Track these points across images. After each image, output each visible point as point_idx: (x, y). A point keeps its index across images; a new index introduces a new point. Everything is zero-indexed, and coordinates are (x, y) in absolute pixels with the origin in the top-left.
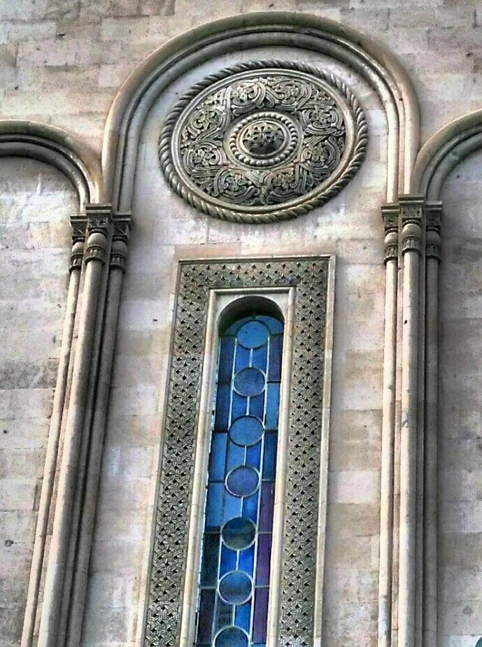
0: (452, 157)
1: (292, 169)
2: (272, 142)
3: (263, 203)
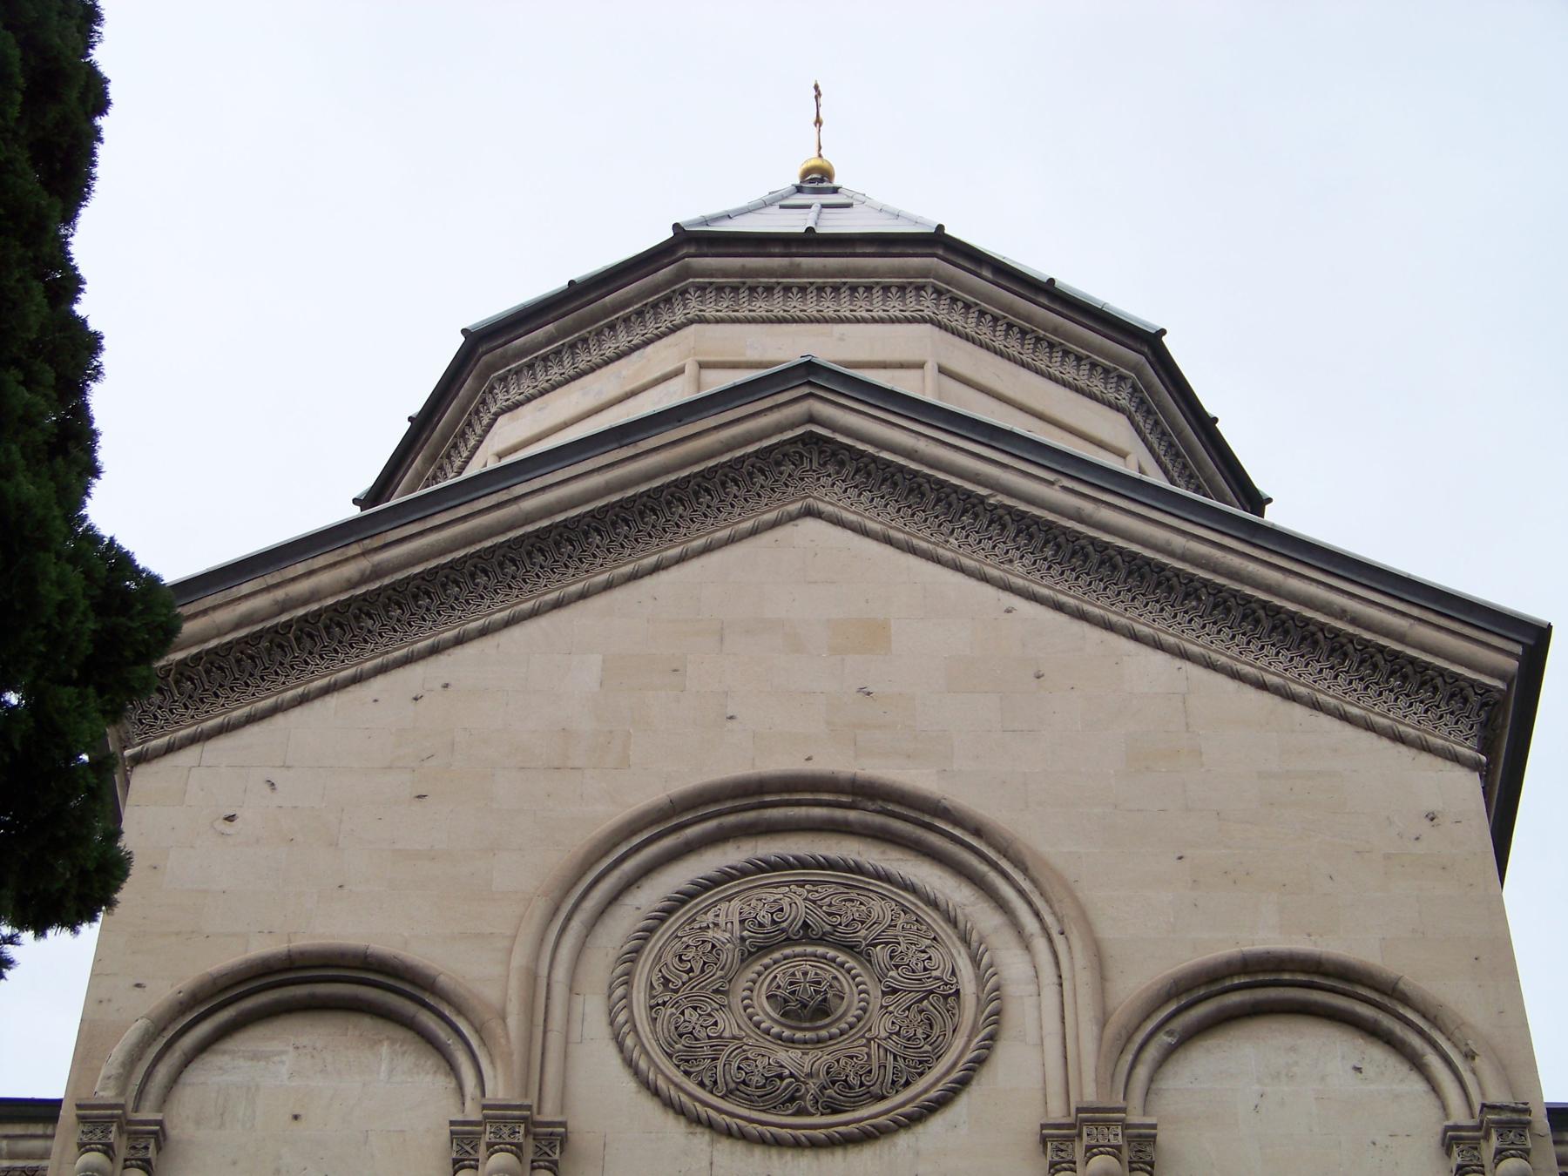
0: (1164, 1039)
1: (866, 1050)
2: (825, 1000)
3: (812, 1111)
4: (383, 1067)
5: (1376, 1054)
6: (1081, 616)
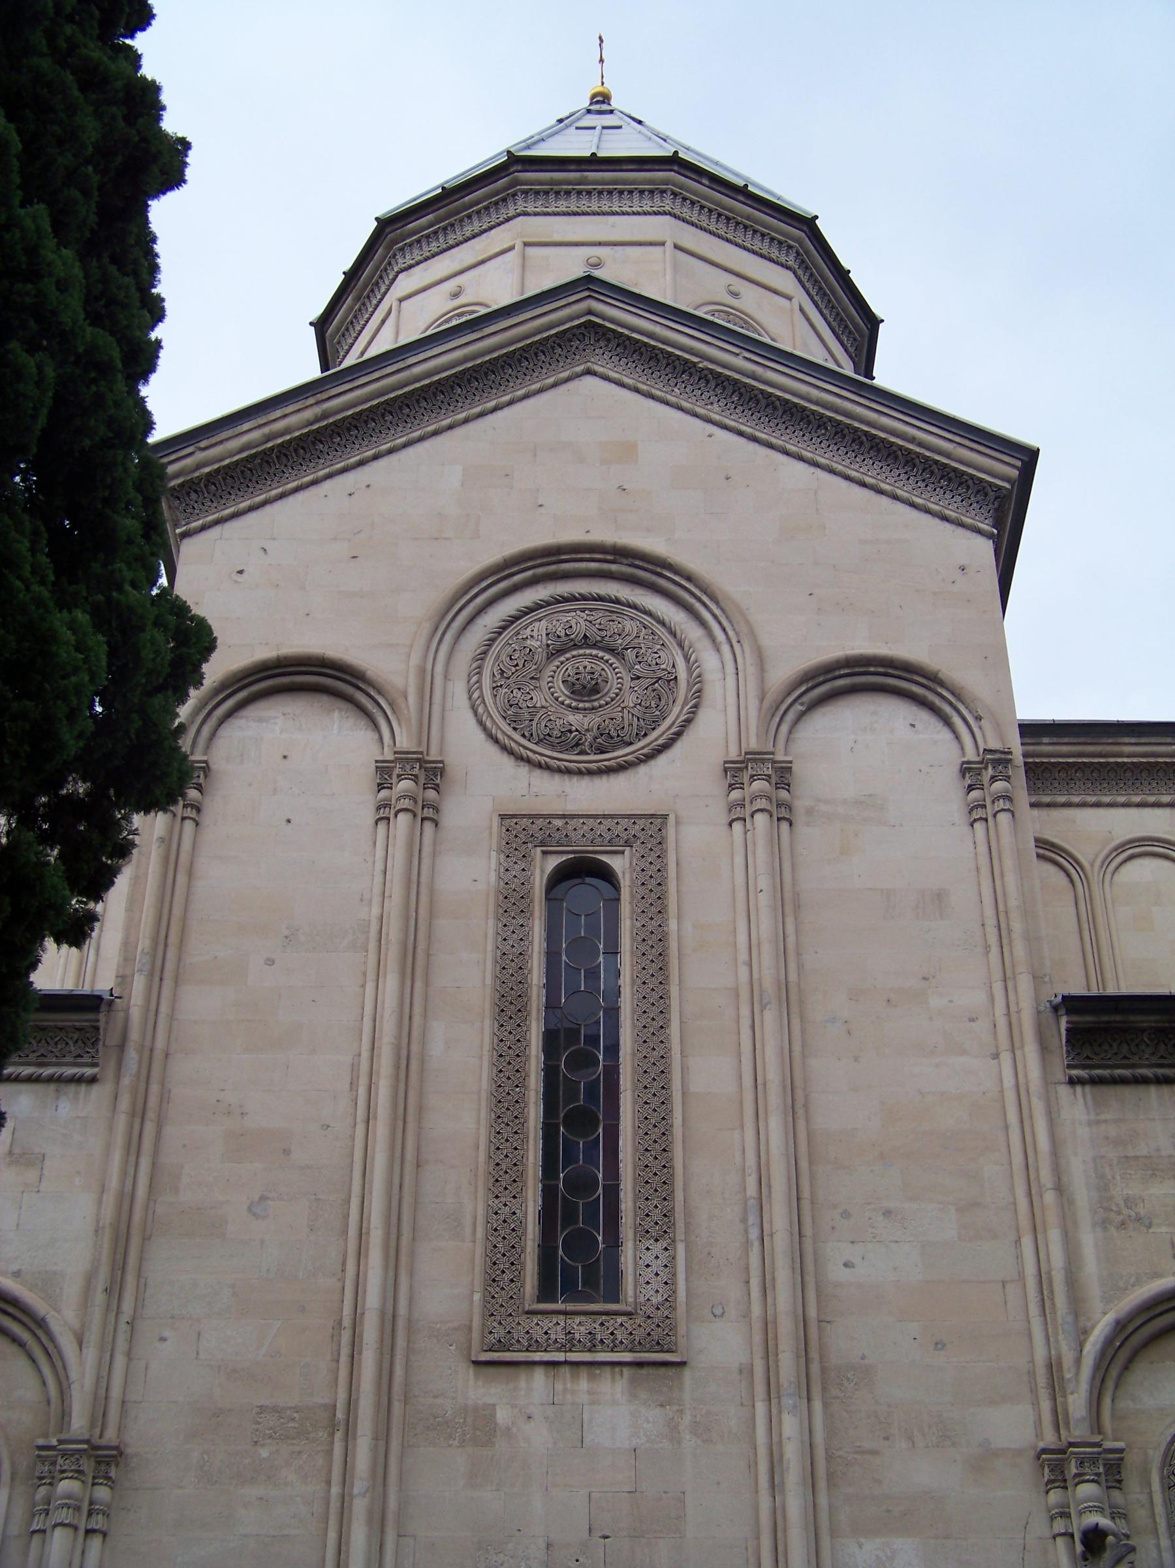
0: (798, 708)
1: (621, 714)
3: (589, 752)
4: (336, 726)
5: (924, 716)
6: (754, 439)
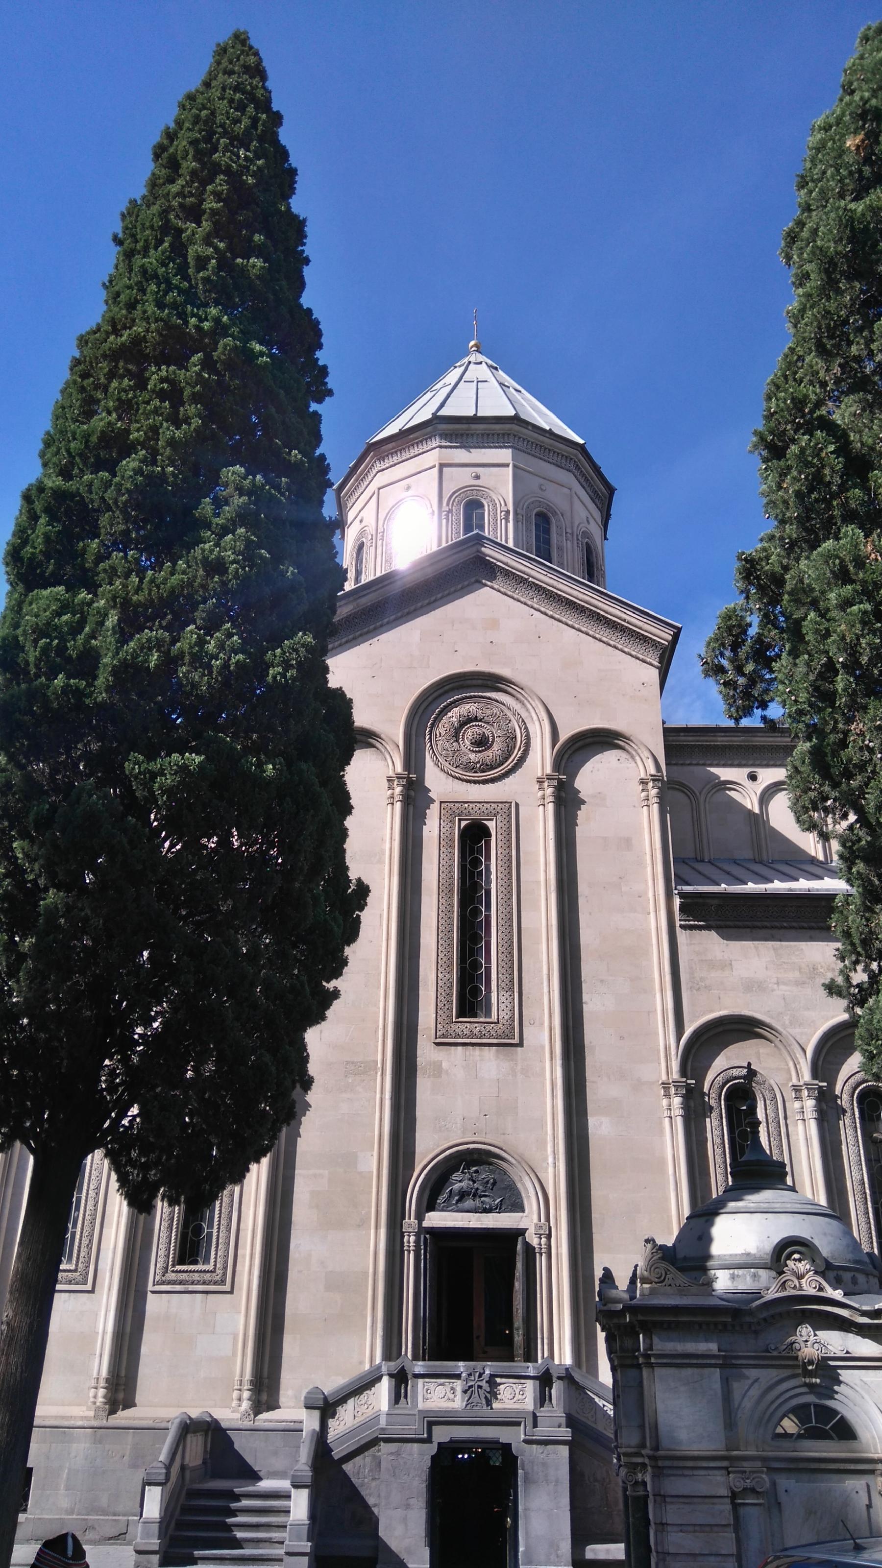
6: (552, 617)
